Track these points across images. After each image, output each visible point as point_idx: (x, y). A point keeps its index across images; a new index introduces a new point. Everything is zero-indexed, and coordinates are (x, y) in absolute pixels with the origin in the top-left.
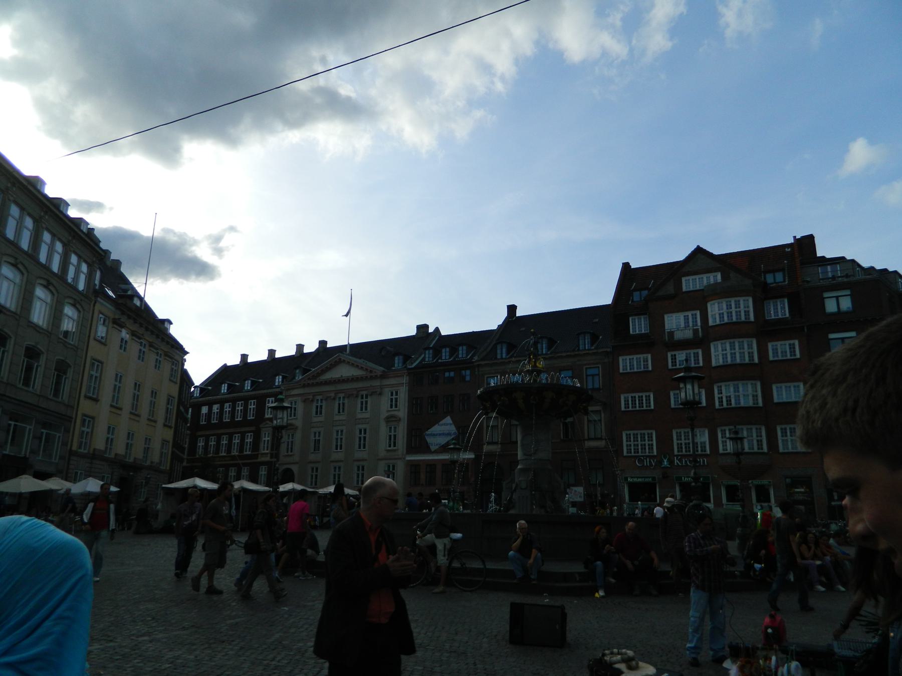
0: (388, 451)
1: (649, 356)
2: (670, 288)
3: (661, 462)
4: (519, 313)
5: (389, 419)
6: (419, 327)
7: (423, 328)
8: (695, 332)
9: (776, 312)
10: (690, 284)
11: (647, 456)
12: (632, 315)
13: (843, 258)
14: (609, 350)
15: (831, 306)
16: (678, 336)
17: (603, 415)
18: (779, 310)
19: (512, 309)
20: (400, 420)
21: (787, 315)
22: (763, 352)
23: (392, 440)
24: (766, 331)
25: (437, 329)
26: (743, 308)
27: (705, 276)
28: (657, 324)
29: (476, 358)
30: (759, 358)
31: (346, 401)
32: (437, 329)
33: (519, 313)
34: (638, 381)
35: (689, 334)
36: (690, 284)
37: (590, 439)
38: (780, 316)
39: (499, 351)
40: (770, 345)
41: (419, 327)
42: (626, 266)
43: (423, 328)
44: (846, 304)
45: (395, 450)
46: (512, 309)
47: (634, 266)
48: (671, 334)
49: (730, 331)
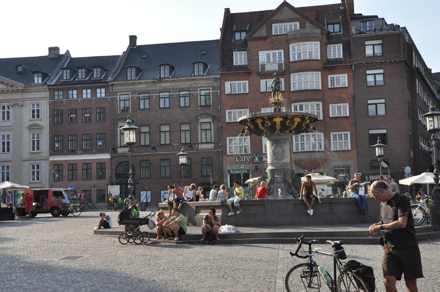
0: (32, 153)
1: (247, 82)
2: (263, 32)
3: (253, 159)
4: (139, 43)
5: (32, 127)
6: (51, 49)
7: (54, 50)
8: (280, 65)
9: (335, 54)
10: (278, 28)
11: (244, 155)
12: (235, 51)
13: (376, 17)
14: (218, 76)
15: (369, 51)
16: (268, 68)
17: (212, 124)
18: (336, 51)
19: (133, 39)
20: (42, 128)
21: (342, 57)
22: (324, 82)
23: (36, 145)
24: (328, 66)
25: (68, 52)
26: (311, 50)
27: (288, 24)
28: (253, 58)
29: (110, 79)
30: (322, 86)
31: (11, 110)
32: (68, 52)
33: (139, 43)
34: (238, 101)
35: (275, 67)
36: (278, 28)
37: (202, 143)
38: (337, 57)
39: (129, 74)
40: (329, 77)
41: (51, 49)
42: (227, 11)
43: (54, 50)
44: (378, 50)
45: (39, 153)
46: (133, 39)
47: (233, 11)
48: (263, 66)
49: (305, 66)
